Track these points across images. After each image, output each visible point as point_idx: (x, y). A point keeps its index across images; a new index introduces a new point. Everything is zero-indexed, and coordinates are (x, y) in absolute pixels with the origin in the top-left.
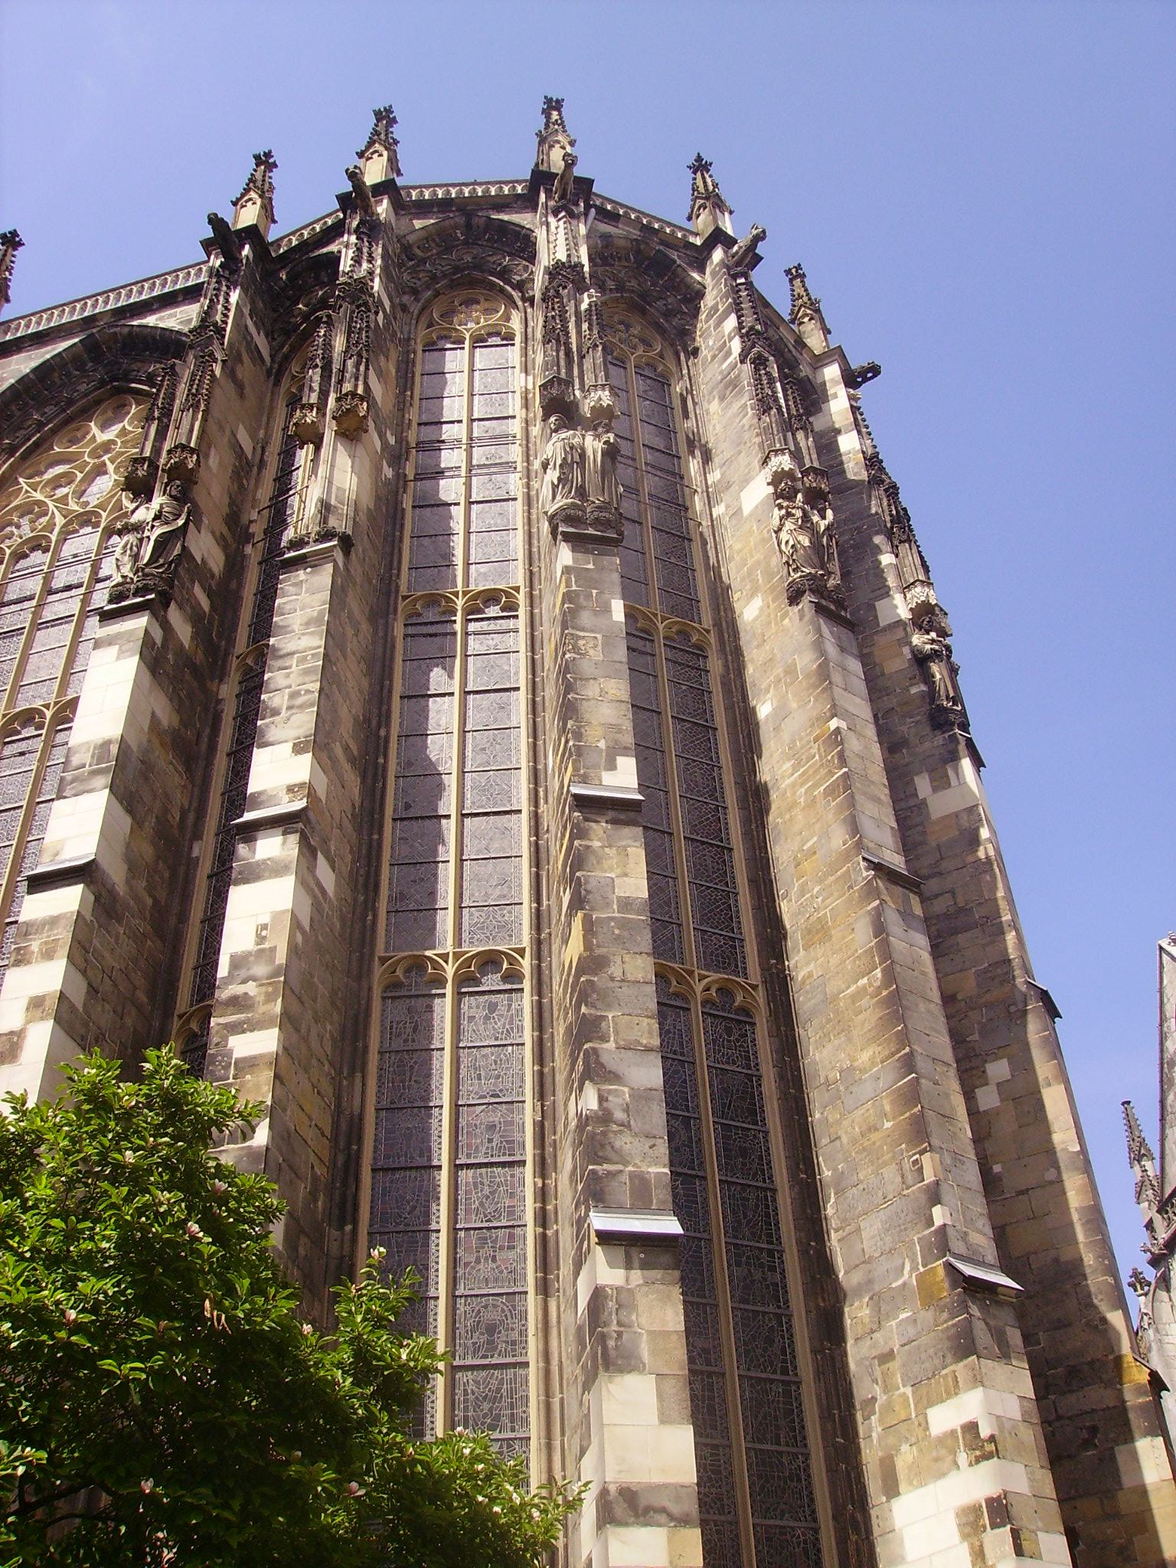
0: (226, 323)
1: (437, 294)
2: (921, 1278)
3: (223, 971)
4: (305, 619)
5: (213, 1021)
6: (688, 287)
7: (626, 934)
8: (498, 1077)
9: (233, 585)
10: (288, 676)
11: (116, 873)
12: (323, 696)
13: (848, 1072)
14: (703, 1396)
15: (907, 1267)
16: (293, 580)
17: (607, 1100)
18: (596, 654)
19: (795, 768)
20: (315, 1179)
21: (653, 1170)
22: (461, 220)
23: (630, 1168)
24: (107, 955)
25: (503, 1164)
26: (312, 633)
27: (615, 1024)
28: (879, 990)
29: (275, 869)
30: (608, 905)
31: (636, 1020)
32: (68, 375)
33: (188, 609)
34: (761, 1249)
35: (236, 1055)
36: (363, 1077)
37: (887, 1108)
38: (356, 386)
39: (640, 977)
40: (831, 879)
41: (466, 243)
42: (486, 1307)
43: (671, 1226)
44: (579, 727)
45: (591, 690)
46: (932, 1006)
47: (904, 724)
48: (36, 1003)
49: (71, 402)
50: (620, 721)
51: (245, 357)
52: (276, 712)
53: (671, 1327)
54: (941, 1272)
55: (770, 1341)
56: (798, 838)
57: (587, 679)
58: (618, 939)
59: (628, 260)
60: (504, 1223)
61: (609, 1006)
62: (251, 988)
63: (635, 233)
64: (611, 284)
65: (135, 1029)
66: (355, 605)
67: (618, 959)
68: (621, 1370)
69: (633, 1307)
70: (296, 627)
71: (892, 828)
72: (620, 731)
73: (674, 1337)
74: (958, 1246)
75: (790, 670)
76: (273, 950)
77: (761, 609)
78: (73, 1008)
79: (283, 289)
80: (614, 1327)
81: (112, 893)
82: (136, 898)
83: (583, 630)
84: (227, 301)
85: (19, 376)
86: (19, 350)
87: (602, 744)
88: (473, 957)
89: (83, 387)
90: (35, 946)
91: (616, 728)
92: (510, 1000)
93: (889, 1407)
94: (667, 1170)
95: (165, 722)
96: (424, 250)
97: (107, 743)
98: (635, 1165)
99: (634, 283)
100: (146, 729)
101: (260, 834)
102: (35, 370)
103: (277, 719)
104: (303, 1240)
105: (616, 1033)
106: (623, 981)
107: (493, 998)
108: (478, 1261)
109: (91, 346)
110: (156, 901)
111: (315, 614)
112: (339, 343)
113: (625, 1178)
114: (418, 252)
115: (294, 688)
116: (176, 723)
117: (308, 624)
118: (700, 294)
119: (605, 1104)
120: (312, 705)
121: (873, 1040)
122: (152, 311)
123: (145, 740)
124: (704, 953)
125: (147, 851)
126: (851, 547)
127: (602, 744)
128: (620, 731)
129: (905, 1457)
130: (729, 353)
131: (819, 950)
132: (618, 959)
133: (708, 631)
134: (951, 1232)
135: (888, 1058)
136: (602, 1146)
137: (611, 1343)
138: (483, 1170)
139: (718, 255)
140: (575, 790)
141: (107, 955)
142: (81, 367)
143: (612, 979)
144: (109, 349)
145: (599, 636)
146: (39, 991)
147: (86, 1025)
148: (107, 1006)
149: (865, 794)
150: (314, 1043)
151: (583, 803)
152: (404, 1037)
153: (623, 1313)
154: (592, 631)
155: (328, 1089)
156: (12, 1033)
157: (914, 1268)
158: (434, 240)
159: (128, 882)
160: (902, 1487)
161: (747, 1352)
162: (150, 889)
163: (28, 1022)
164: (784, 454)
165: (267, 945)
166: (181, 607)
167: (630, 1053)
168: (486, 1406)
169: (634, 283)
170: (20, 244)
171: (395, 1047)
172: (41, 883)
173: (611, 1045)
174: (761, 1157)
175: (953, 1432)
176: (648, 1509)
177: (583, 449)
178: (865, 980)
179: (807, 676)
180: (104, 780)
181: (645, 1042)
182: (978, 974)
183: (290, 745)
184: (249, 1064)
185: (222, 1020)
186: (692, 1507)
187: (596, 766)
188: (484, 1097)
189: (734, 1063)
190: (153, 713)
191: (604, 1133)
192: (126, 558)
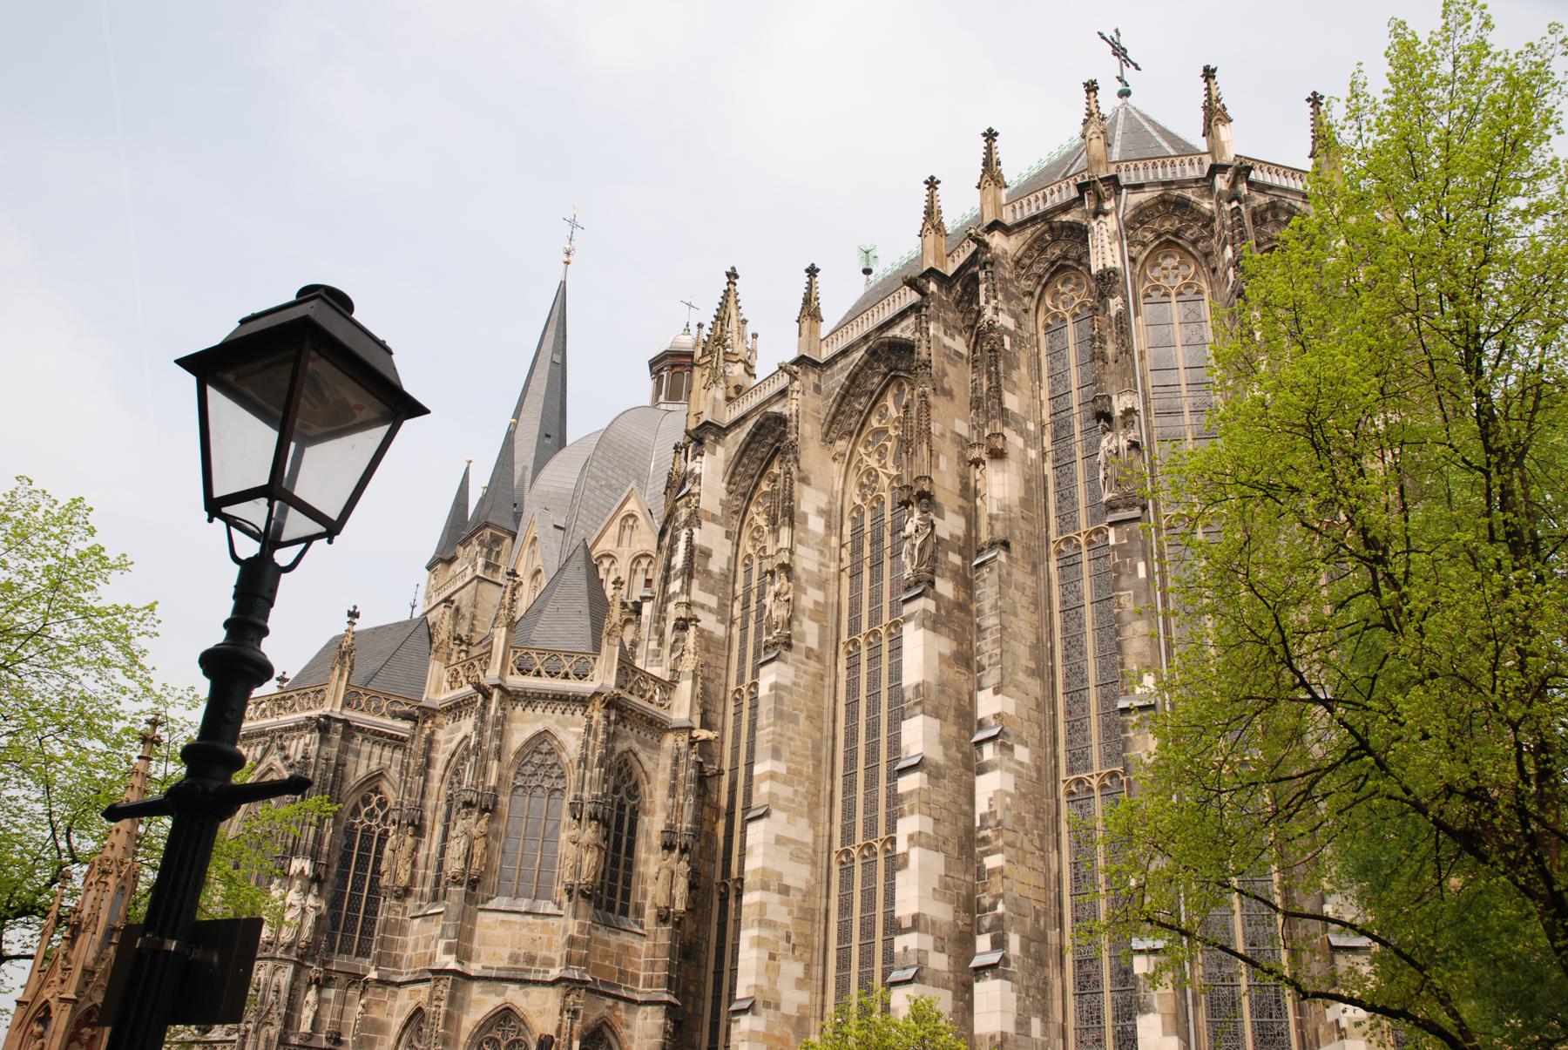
1: (1045, 286)
3: (978, 824)
5: (977, 850)
6: (1203, 215)
9: (973, 535)
11: (936, 755)
18: (1130, 606)
20: (1037, 913)
33: (948, 574)
35: (988, 867)
36: (1059, 853)
41: (1053, 241)
45: (1128, 632)
48: (911, 838)
49: (872, 393)
52: (984, 669)
59: (1158, 211)
62: (988, 833)
63: (1158, 192)
64: (1150, 236)
66: (1020, 575)
68: (1146, 1013)
72: (1144, 657)
78: (928, 836)
81: (937, 767)
83: (1122, 590)
87: (1135, 668)
89: (876, 380)
90: (906, 807)
96: (1031, 257)
99: (1167, 225)
102: (847, 378)
109: (872, 353)
110: (964, 753)
116: (954, 645)
123: (938, 673)
125: (952, 730)
127: (1135, 668)
128: (1144, 657)
130: (1228, 283)
142: (871, 368)
147: (937, 839)
150: (1027, 846)
155: (1039, 864)
159: (945, 755)
162: (958, 750)
166: (942, 577)
170: (818, 270)
177: (1117, 448)
184: (992, 872)
190: (940, 654)
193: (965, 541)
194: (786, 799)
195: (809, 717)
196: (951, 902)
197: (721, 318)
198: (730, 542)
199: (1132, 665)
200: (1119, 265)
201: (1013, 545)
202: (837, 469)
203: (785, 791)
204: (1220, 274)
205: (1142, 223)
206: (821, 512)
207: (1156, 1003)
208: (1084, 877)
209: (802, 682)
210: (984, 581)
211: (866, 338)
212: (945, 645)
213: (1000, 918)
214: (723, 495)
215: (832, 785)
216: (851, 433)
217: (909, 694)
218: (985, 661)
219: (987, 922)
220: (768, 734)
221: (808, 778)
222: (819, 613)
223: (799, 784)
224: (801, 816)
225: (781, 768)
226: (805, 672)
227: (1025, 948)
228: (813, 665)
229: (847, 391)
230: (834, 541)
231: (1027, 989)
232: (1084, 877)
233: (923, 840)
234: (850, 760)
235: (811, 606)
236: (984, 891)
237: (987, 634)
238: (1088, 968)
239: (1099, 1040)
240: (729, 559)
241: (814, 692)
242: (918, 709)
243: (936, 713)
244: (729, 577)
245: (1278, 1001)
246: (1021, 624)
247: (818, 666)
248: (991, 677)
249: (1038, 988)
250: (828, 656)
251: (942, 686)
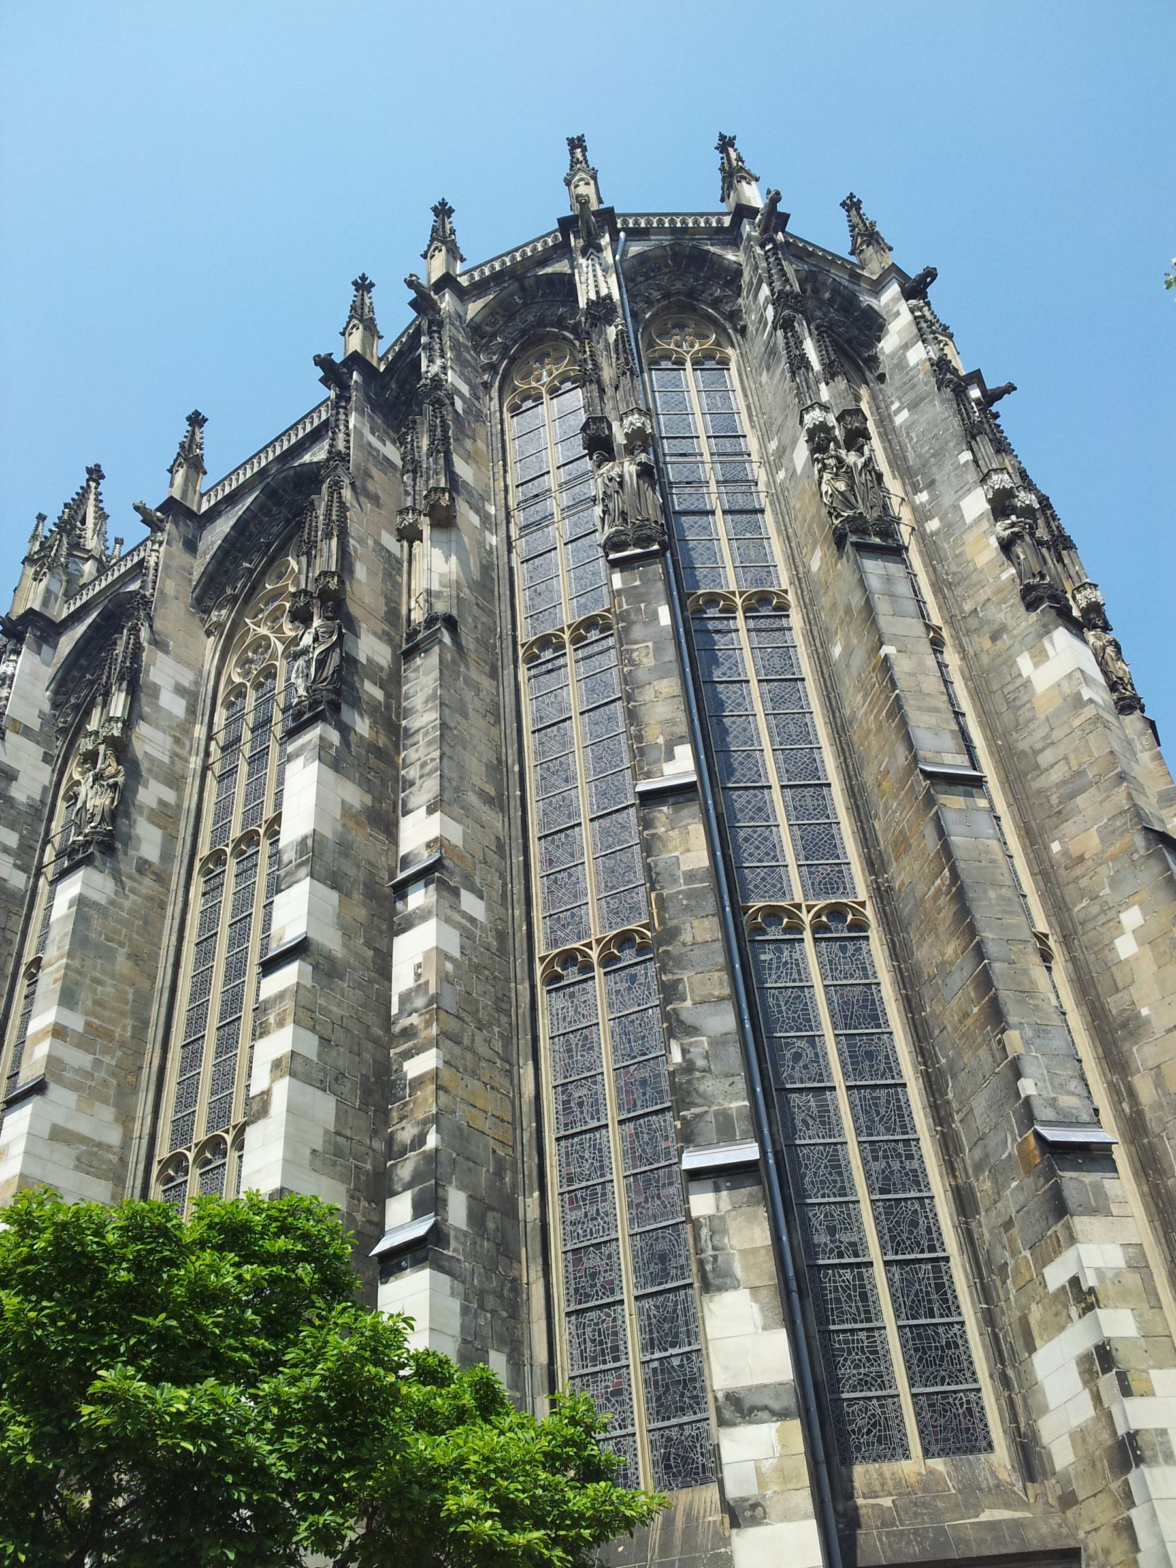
0: (348, 448)
1: (513, 360)
3: (395, 1010)
4: (424, 699)
7: (693, 903)
8: (643, 1038)
10: (417, 750)
11: (331, 940)
12: (445, 760)
13: (941, 965)
14: (855, 1286)
16: (413, 667)
17: (689, 1051)
18: (649, 661)
19: (865, 697)
21: (734, 1105)
22: (515, 286)
23: (715, 1108)
24: (334, 1009)
25: (656, 1112)
26: (430, 709)
27: (690, 983)
29: (422, 915)
30: (675, 881)
31: (707, 975)
32: (261, 523)
34: (896, 1141)
35: (409, 1077)
37: (973, 994)
38: (438, 481)
39: (708, 937)
40: (903, 793)
41: (525, 305)
42: (657, 1239)
43: (749, 1152)
44: (640, 731)
45: (647, 695)
46: (1004, 891)
47: (1001, 611)
48: (277, 1065)
49: (269, 545)
50: (674, 715)
51: (375, 472)
52: (412, 784)
53: (758, 1244)
54: (1032, 1141)
55: (914, 1224)
56: (876, 762)
57: (643, 686)
58: (687, 909)
59: (667, 266)
60: (663, 1163)
62: (415, 1019)
63: (666, 240)
64: (656, 295)
65: (374, 1060)
67: (688, 926)
68: (720, 1289)
69: (725, 1232)
70: (418, 707)
71: (952, 731)
72: (675, 724)
73: (763, 1252)
74: (1043, 1112)
75: (848, 610)
76: (427, 983)
77: (821, 559)
78: (307, 1061)
79: (397, 398)
80: (710, 1252)
81: (329, 958)
82: (357, 955)
83: (636, 643)
84: (347, 427)
85: (223, 536)
86: (220, 514)
88: (611, 939)
89: (275, 530)
90: (272, 1019)
91: (672, 722)
92: (646, 968)
93: (1017, 1270)
94: (746, 1103)
95: (357, 805)
96: (493, 324)
97: (305, 838)
98: (719, 1104)
99: (678, 285)
100: (338, 816)
101: (410, 889)
102: (232, 528)
103: (414, 789)
104: (490, 1215)
105: (692, 991)
106: (693, 944)
107: (632, 970)
108: (646, 1201)
109: (272, 495)
110: (376, 950)
111: (431, 691)
112: (425, 443)
113: (710, 1117)
114: (488, 329)
115: (423, 759)
116: (368, 800)
117: (426, 702)
118: (739, 273)
119: (688, 1056)
120: (436, 770)
121: (952, 934)
122: (307, 450)
123: (339, 828)
124: (813, 884)
125: (362, 913)
126: (933, 456)
127: (661, 740)
129: (1036, 1314)
130: (766, 324)
131: (906, 860)
132: (688, 926)
133: (786, 592)
134: (1036, 1104)
135: (965, 949)
136: (689, 1093)
137: (709, 1267)
138: (642, 1121)
139: (746, 228)
140: (640, 788)
141: (334, 1009)
142: (268, 514)
143: (684, 944)
144: (285, 491)
145: (650, 644)
146: (277, 1055)
148: (342, 1049)
149: (919, 708)
150: (482, 1049)
151: (650, 798)
152: (568, 1019)
153: (717, 1237)
154: (644, 641)
155: (502, 1082)
156: (262, 1093)
157: (1014, 1140)
158: (497, 313)
159: (344, 945)
160: (1038, 1343)
161: (892, 1238)
162: (368, 944)
163: (273, 1081)
164: (814, 409)
165: (422, 981)
167: (705, 1006)
168: (666, 1326)
169: (678, 285)
170: (205, 420)
171: (562, 1031)
172: (270, 966)
174: (887, 1057)
175: (1064, 1287)
176: (753, 1409)
178: (938, 882)
179: (859, 613)
180: (304, 871)
181: (717, 993)
182: (1099, 831)
183: (424, 808)
185: (398, 1050)
186: (790, 1401)
187: (658, 761)
188: (635, 1057)
189: (852, 976)
190: (343, 802)
191: (689, 1082)
192: (300, 681)
193: (390, 675)
194: (78, 1071)
195: (134, 957)
196: (343, 1179)
197: (76, 508)
198: (49, 768)
199: (656, 737)
200: (616, 296)
201: (462, 629)
202: (210, 647)
203: (80, 1059)
204: (751, 329)
205: (648, 278)
206: (180, 690)
207: (738, 1268)
208: (581, 1105)
209: (127, 904)
210: (417, 669)
211: (263, 472)
212: (354, 795)
214: (47, 707)
215: (164, 1059)
216: (235, 598)
217: (289, 856)
218: (412, 773)
219: (405, 1171)
220: (58, 970)
221: (122, 1044)
222: (165, 816)
223: (105, 1052)
224: (105, 1101)
225: (76, 1022)
226: (132, 891)
227: (476, 1216)
228: (148, 884)
229: (233, 545)
230: (200, 731)
231: (481, 1294)
232: (581, 1105)
233: (299, 1067)
234: (197, 1020)
235: (154, 805)
236: (401, 1119)
237: (419, 737)
238: (592, 1261)
239: (618, 1392)
240: (45, 789)
241: (146, 922)
242: (304, 871)
243: (334, 881)
244: (41, 812)
245: (940, 1287)
246: (473, 731)
247: (156, 886)
248: (425, 791)
249: (500, 1296)
250: (175, 877)
251: (344, 847)
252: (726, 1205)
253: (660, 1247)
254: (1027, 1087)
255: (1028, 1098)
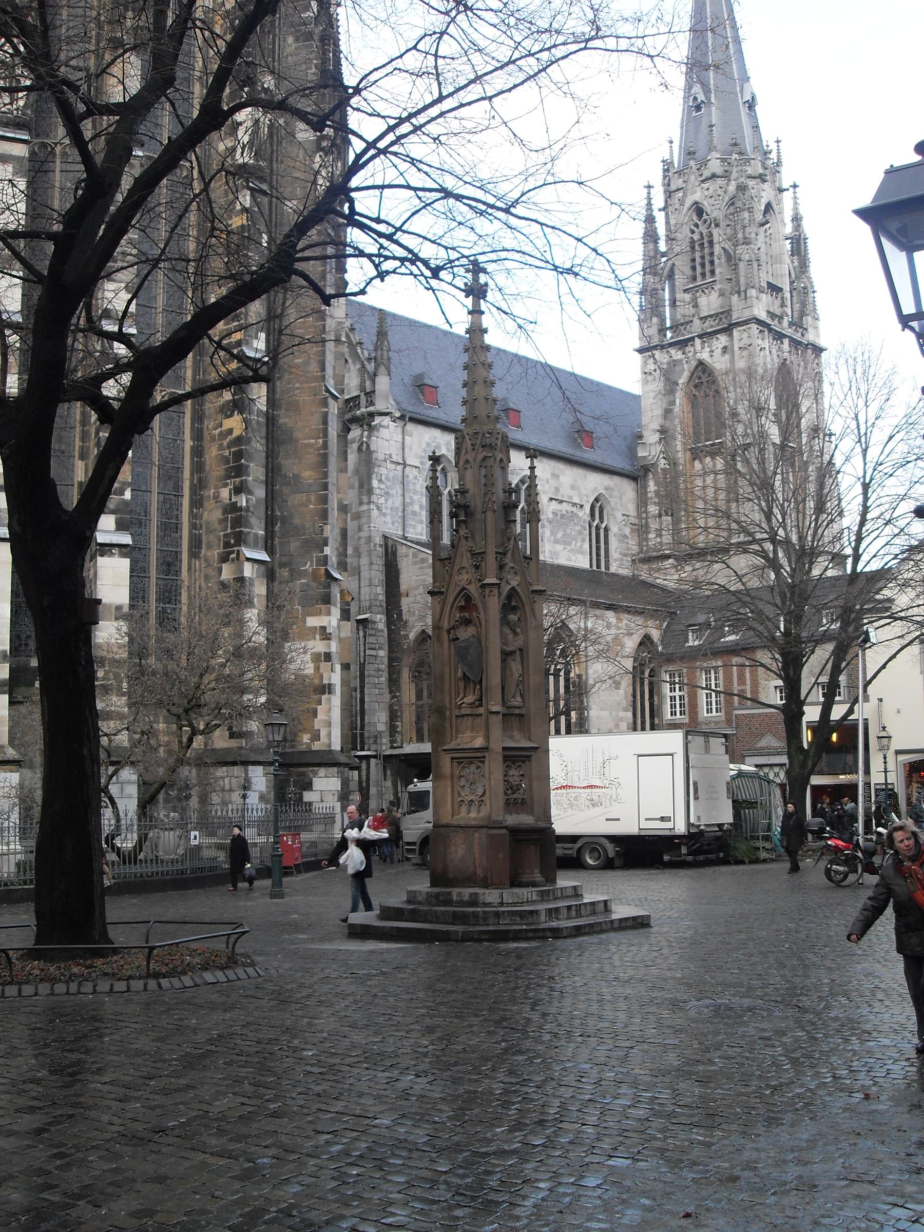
2: (313, 570)
15: (309, 564)
28: (318, 449)
37: (313, 500)
54: (323, 572)
61: (251, 461)
157: (311, 565)
173: (250, 479)
213: (126, 503)
252: (255, 576)
253: (169, 559)
254: (327, 551)
255: (327, 556)
